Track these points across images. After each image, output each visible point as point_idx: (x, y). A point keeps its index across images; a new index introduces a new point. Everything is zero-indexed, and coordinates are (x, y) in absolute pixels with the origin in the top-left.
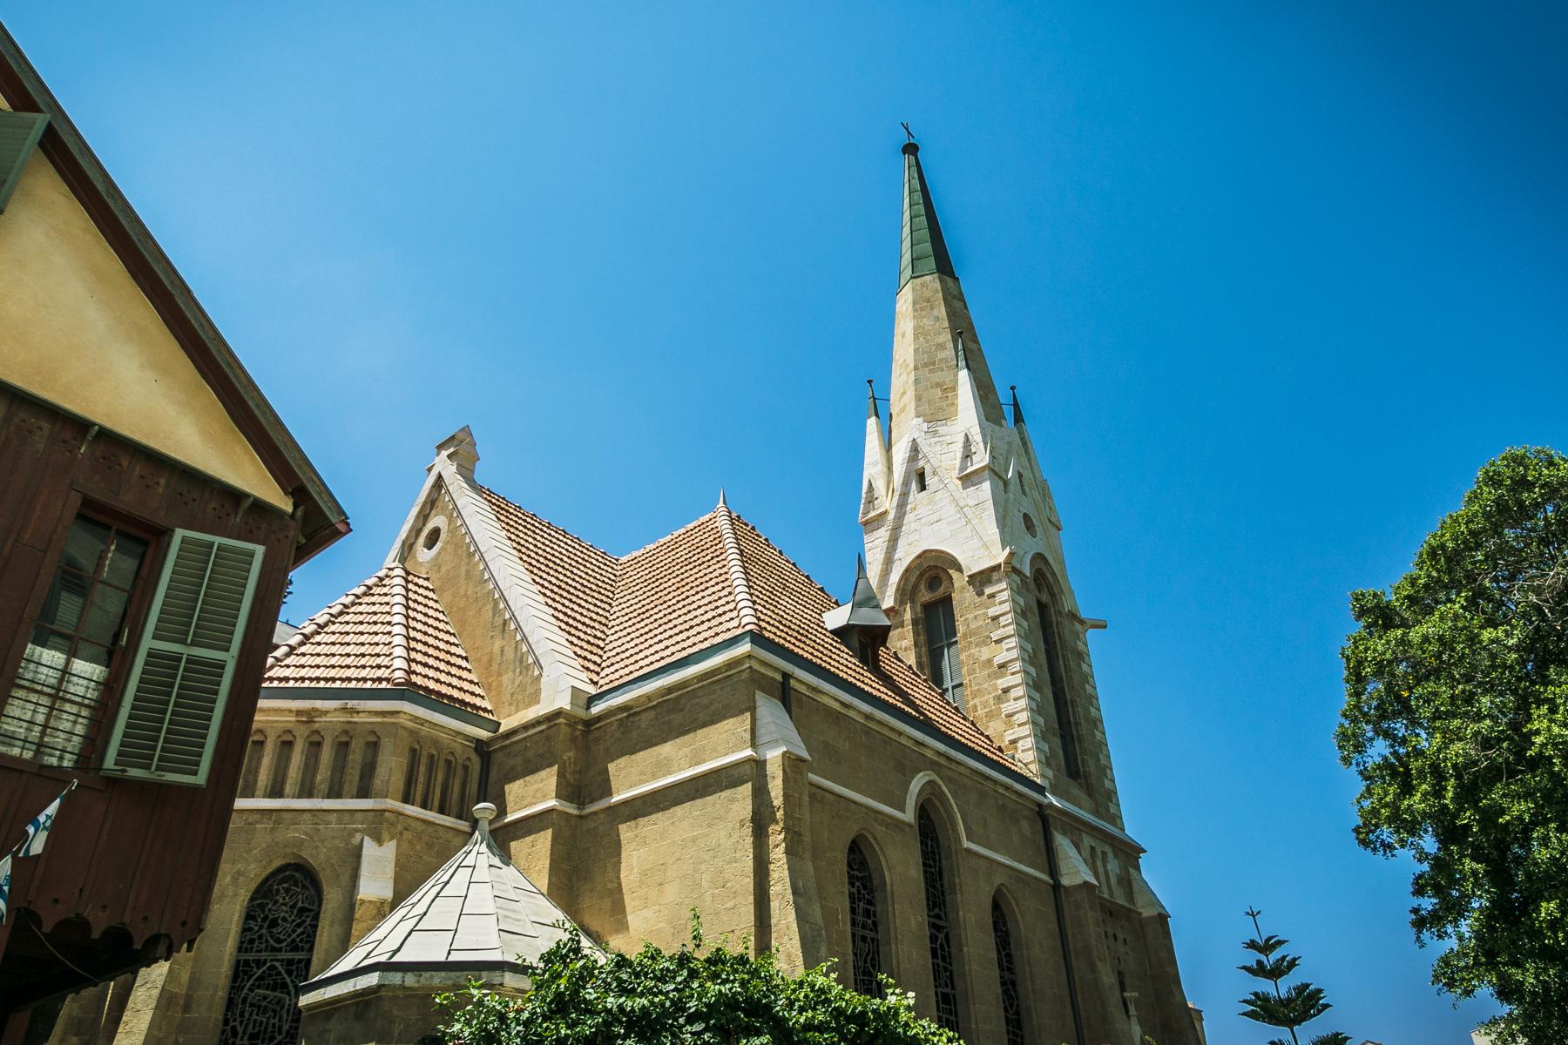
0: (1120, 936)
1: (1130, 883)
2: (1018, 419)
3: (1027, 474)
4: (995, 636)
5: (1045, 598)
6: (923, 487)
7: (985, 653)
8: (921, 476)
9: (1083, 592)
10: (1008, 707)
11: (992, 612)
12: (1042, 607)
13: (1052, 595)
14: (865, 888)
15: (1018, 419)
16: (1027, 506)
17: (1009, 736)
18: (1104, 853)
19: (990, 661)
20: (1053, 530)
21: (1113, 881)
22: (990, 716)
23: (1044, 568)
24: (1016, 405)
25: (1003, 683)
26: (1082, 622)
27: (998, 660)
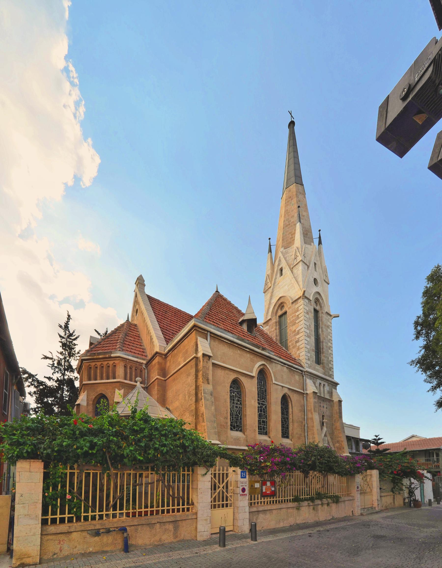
0: (325, 406)
1: (332, 393)
2: (320, 243)
3: (318, 263)
4: (297, 322)
5: (318, 308)
6: (281, 274)
7: (294, 328)
8: (281, 270)
9: (332, 305)
10: (298, 344)
11: (297, 314)
12: (316, 311)
13: (321, 307)
14: (238, 394)
15: (320, 243)
16: (316, 276)
17: (298, 352)
18: (324, 385)
19: (295, 330)
20: (326, 284)
21: (326, 392)
22: (293, 347)
23: (319, 298)
24: (320, 237)
25: (298, 337)
26: (331, 316)
27: (297, 330)
